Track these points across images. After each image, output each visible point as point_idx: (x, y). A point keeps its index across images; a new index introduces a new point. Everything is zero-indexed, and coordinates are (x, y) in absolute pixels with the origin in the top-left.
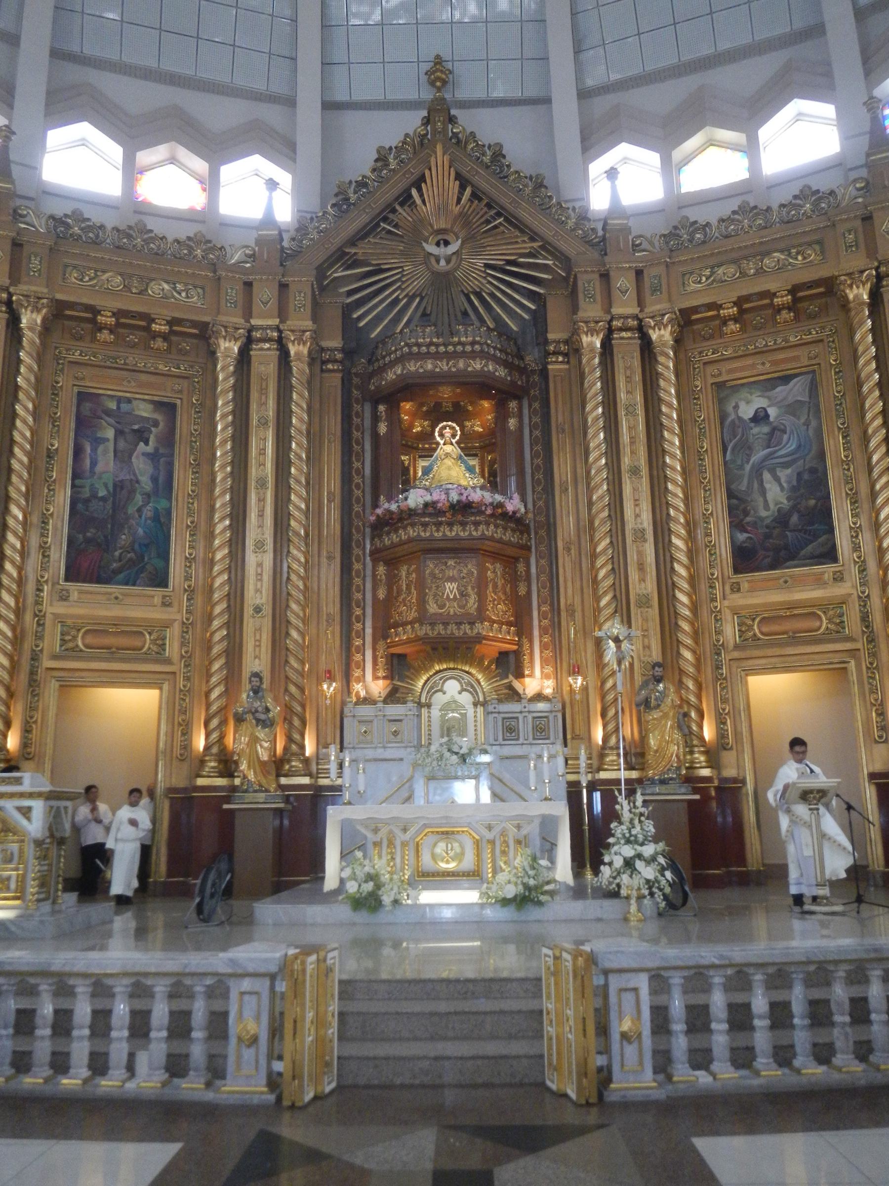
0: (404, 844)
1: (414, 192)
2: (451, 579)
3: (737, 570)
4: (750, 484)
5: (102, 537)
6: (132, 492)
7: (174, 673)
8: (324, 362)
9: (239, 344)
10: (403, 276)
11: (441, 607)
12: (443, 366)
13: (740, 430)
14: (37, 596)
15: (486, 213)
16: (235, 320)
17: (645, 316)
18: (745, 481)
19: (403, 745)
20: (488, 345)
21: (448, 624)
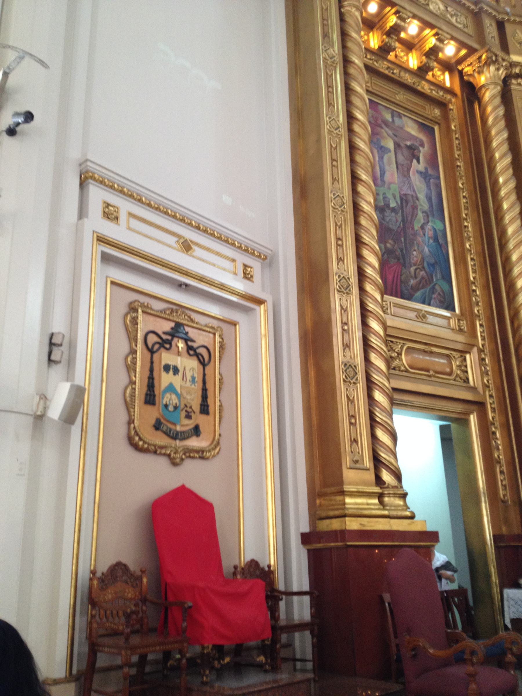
5: (399, 251)
6: (415, 208)
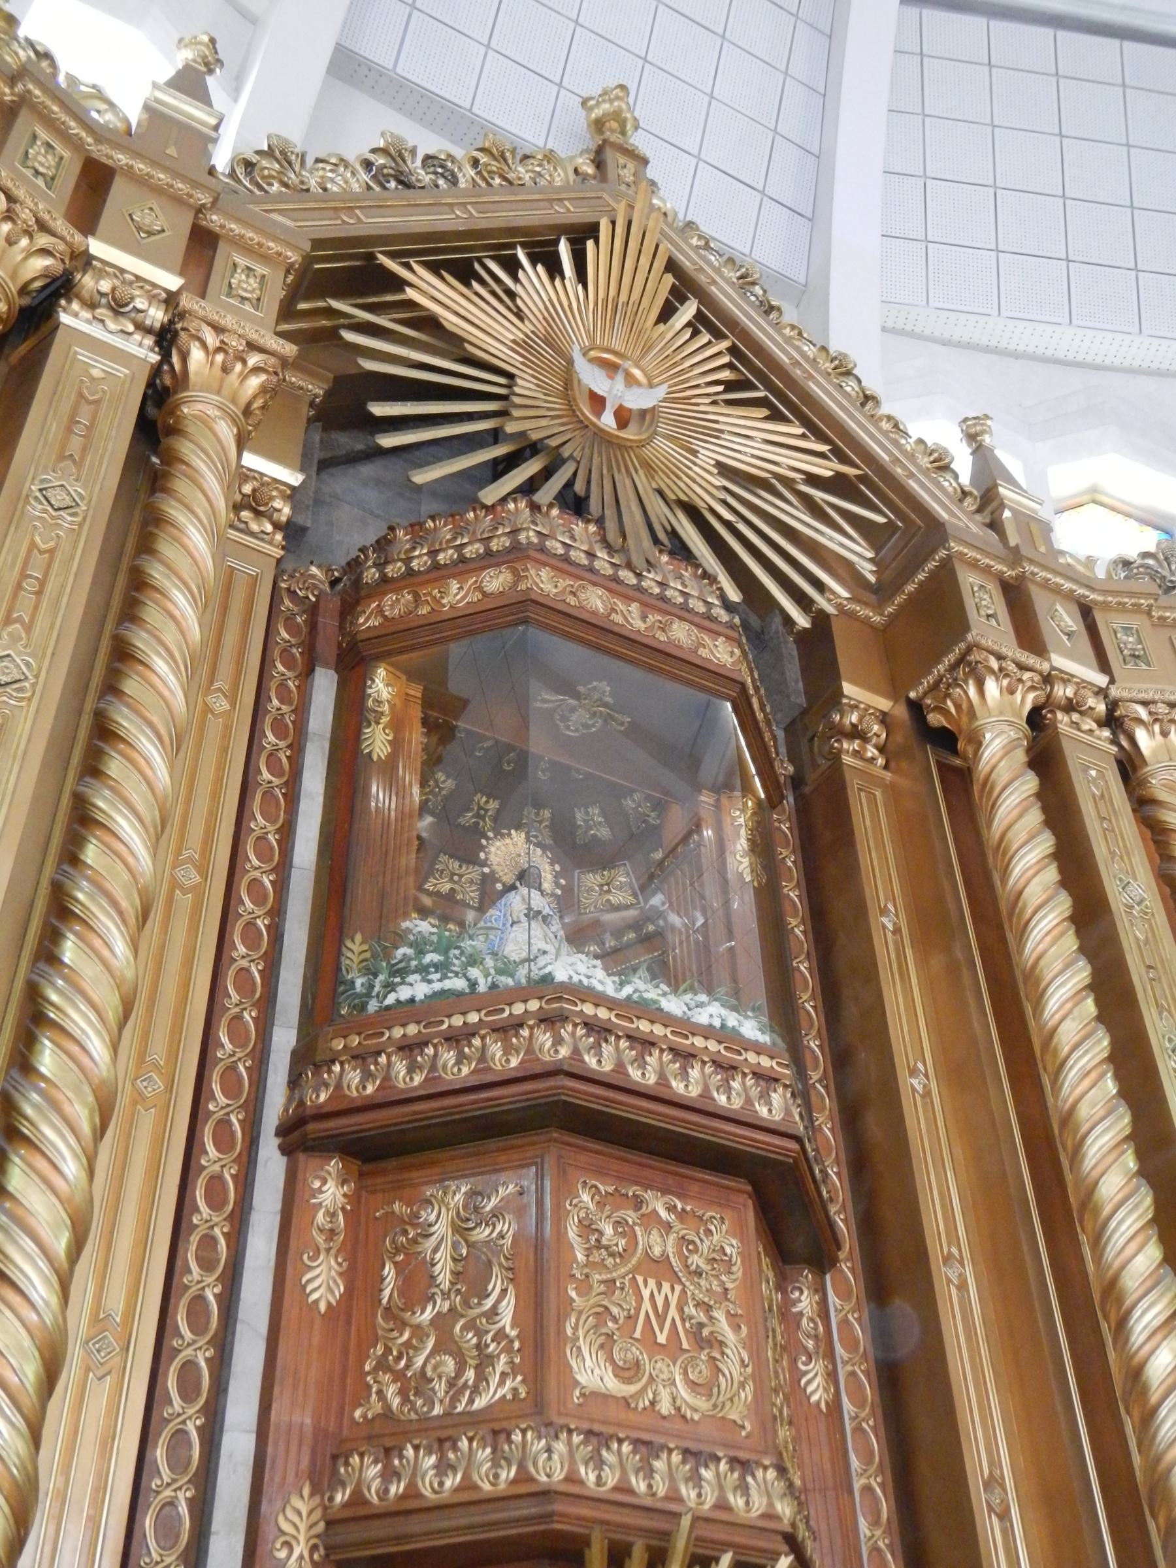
1: (564, 250)
2: (659, 1267)
11: (628, 1372)
17: (1125, 694)
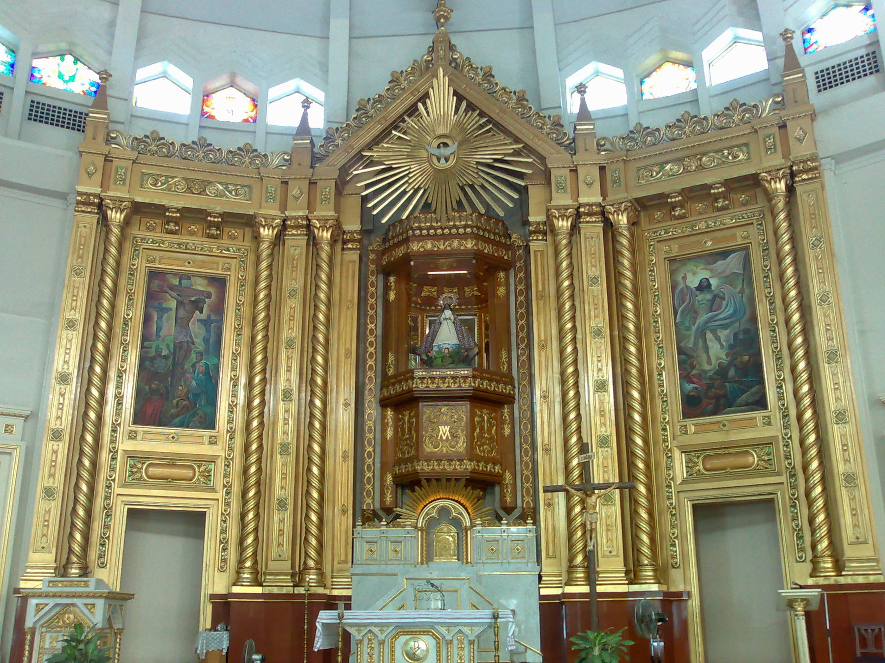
0: (382, 643)
1: (420, 105)
2: (445, 424)
3: (686, 415)
4: (696, 343)
6: (188, 351)
7: (218, 500)
8: (345, 242)
9: (275, 231)
10: (410, 173)
12: (442, 246)
13: (688, 297)
14: (112, 436)
15: (479, 120)
16: (272, 212)
17: (605, 204)
18: (692, 338)
19: (403, 562)
20: (478, 228)
21: (441, 461)
